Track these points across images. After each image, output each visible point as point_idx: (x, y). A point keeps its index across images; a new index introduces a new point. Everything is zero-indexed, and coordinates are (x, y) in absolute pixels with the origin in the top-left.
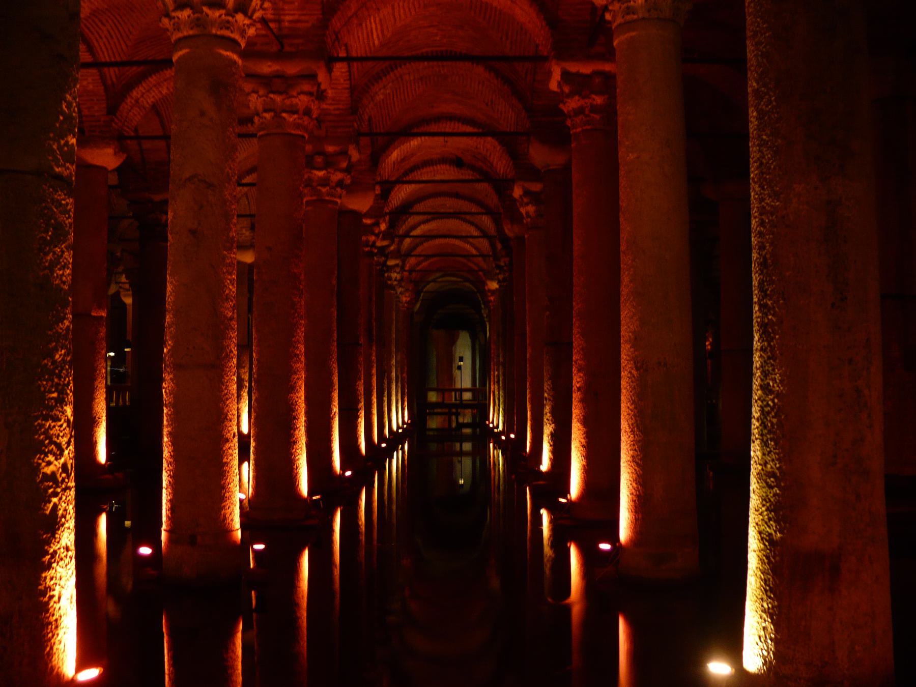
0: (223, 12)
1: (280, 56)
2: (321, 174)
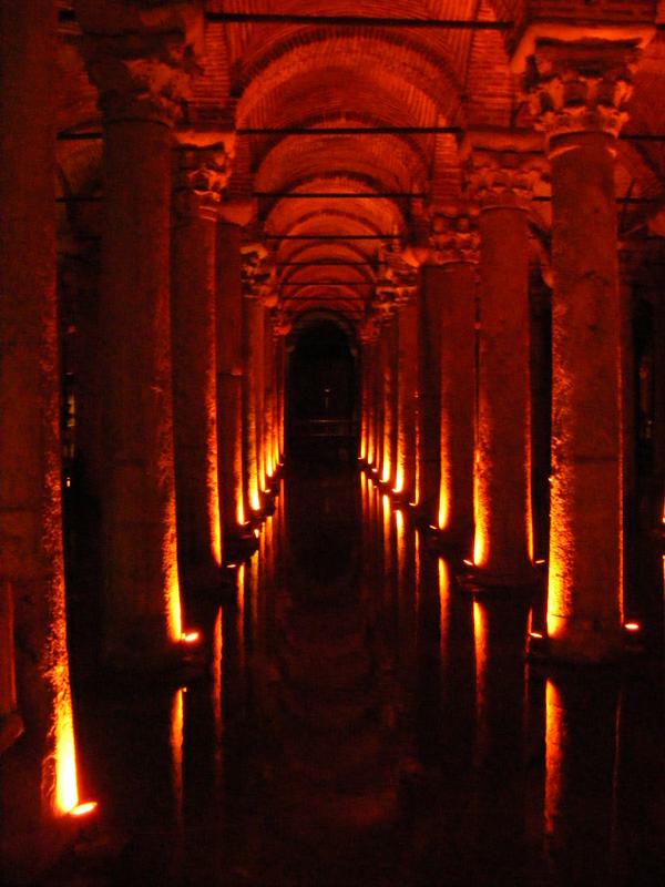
0: (614, 110)
1: (512, 131)
2: (464, 236)
